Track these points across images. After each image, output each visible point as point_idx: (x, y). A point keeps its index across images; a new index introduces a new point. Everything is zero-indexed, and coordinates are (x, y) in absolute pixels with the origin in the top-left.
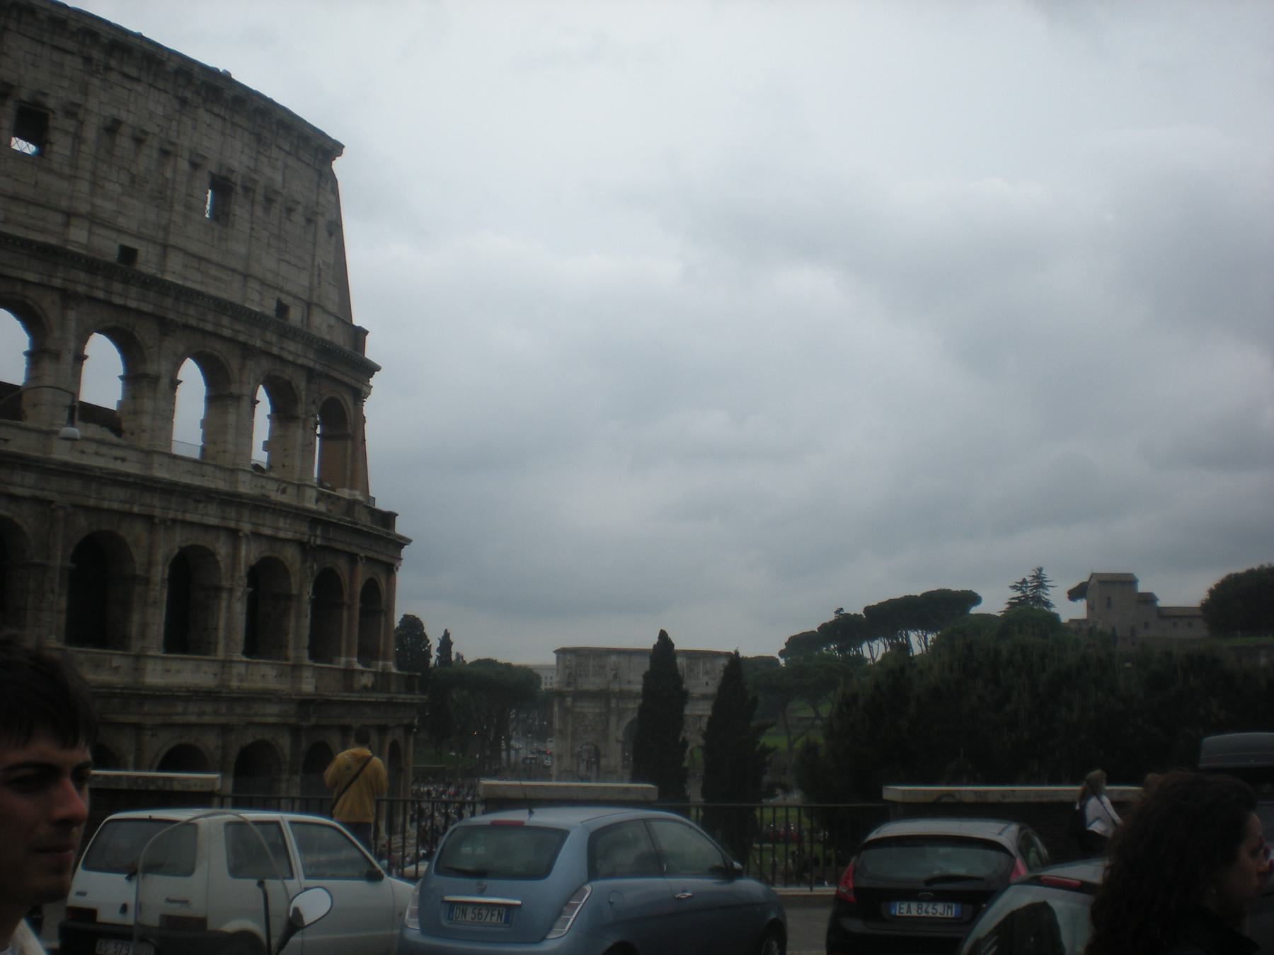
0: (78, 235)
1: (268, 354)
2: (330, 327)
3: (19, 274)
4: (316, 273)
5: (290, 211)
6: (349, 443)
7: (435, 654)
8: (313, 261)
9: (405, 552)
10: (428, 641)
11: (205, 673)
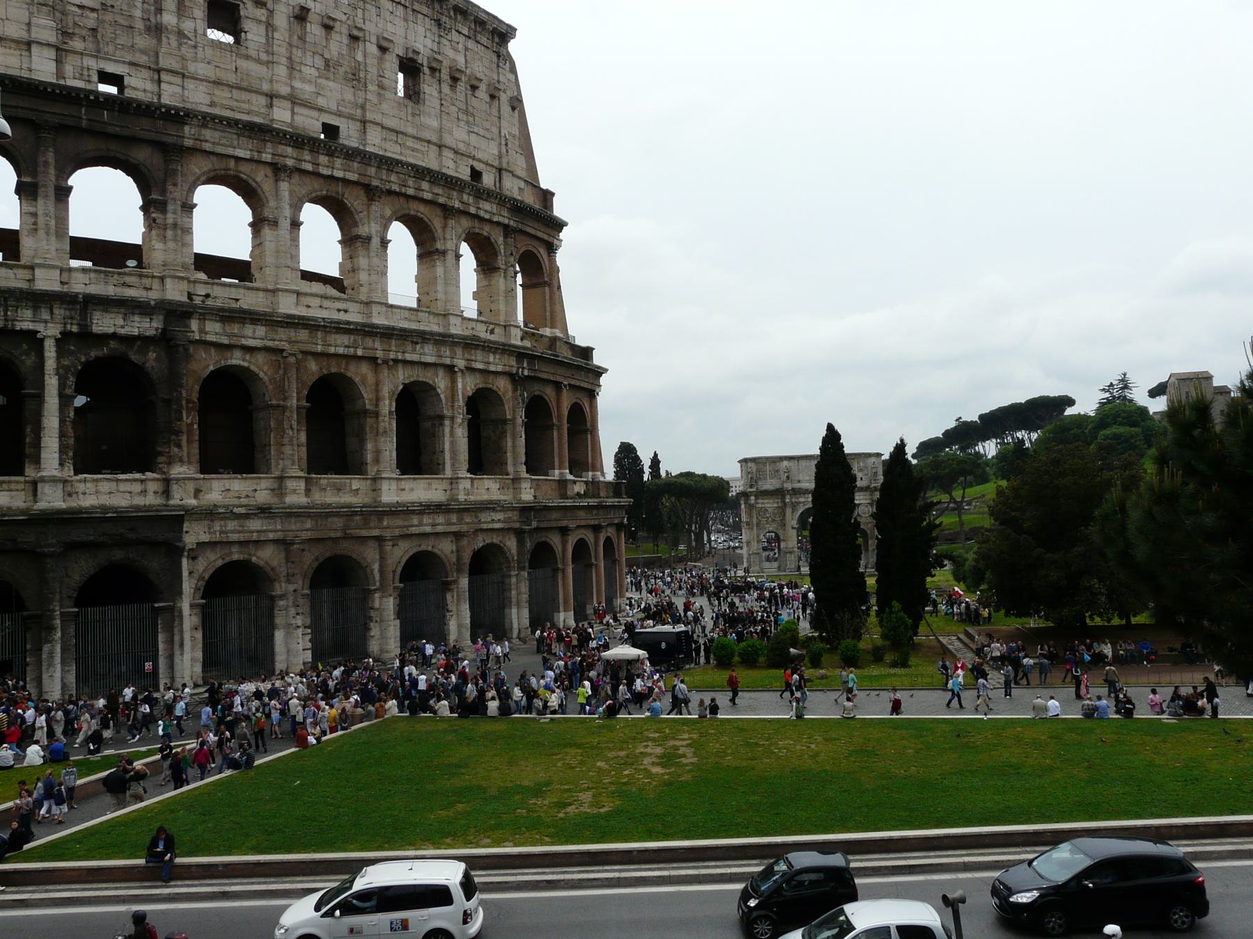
0: (282, 115)
1: (467, 214)
2: (520, 189)
3: (230, 151)
4: (503, 143)
5: (474, 88)
6: (547, 289)
7: (647, 470)
8: (500, 132)
9: (603, 380)
10: (641, 461)
11: (436, 489)
